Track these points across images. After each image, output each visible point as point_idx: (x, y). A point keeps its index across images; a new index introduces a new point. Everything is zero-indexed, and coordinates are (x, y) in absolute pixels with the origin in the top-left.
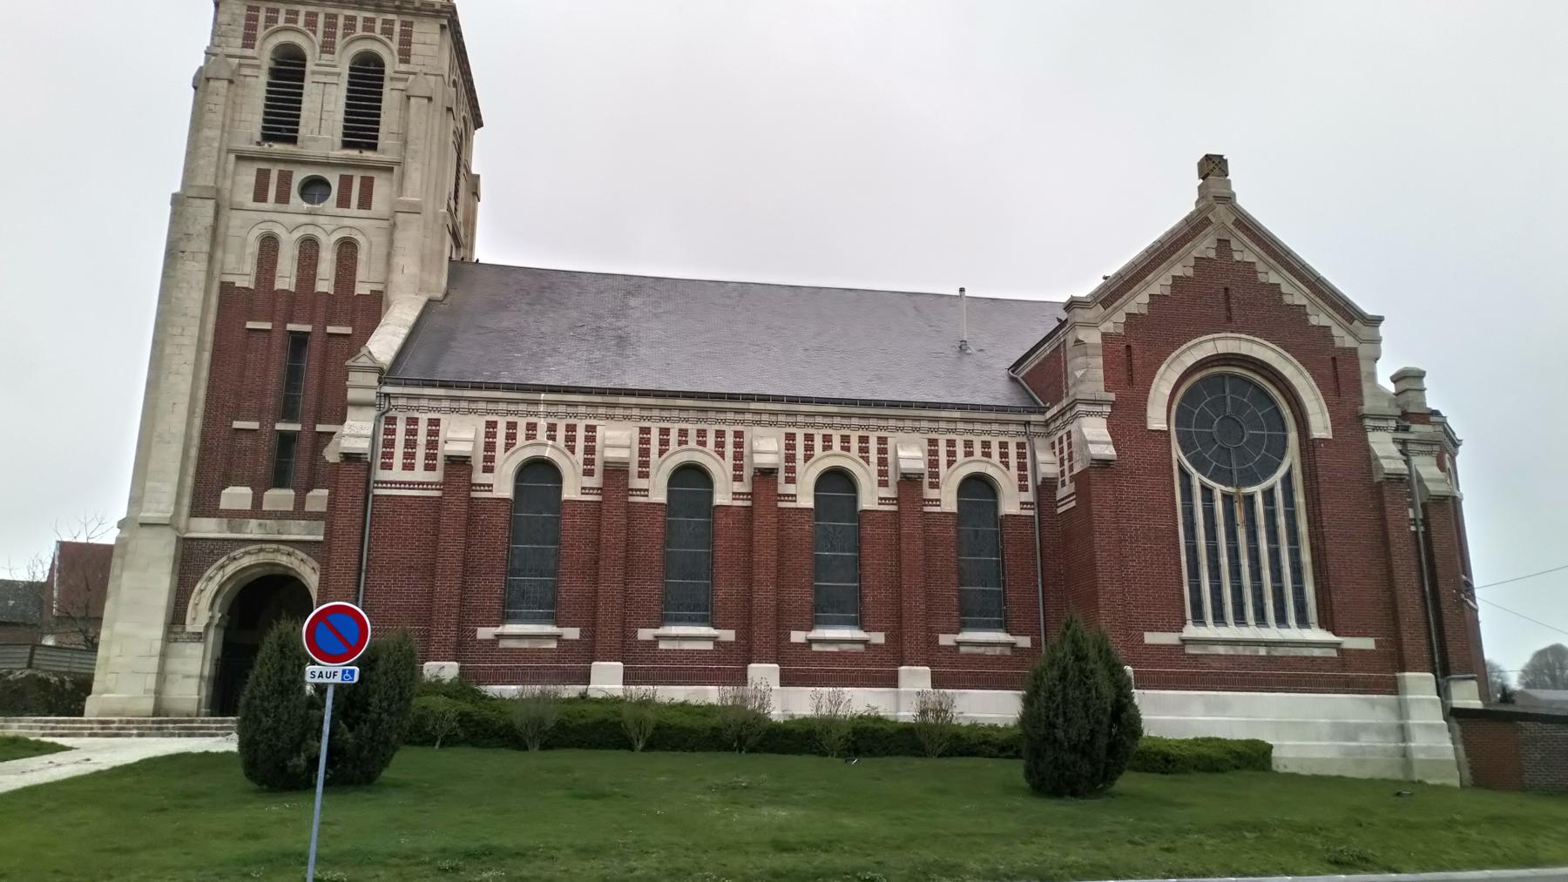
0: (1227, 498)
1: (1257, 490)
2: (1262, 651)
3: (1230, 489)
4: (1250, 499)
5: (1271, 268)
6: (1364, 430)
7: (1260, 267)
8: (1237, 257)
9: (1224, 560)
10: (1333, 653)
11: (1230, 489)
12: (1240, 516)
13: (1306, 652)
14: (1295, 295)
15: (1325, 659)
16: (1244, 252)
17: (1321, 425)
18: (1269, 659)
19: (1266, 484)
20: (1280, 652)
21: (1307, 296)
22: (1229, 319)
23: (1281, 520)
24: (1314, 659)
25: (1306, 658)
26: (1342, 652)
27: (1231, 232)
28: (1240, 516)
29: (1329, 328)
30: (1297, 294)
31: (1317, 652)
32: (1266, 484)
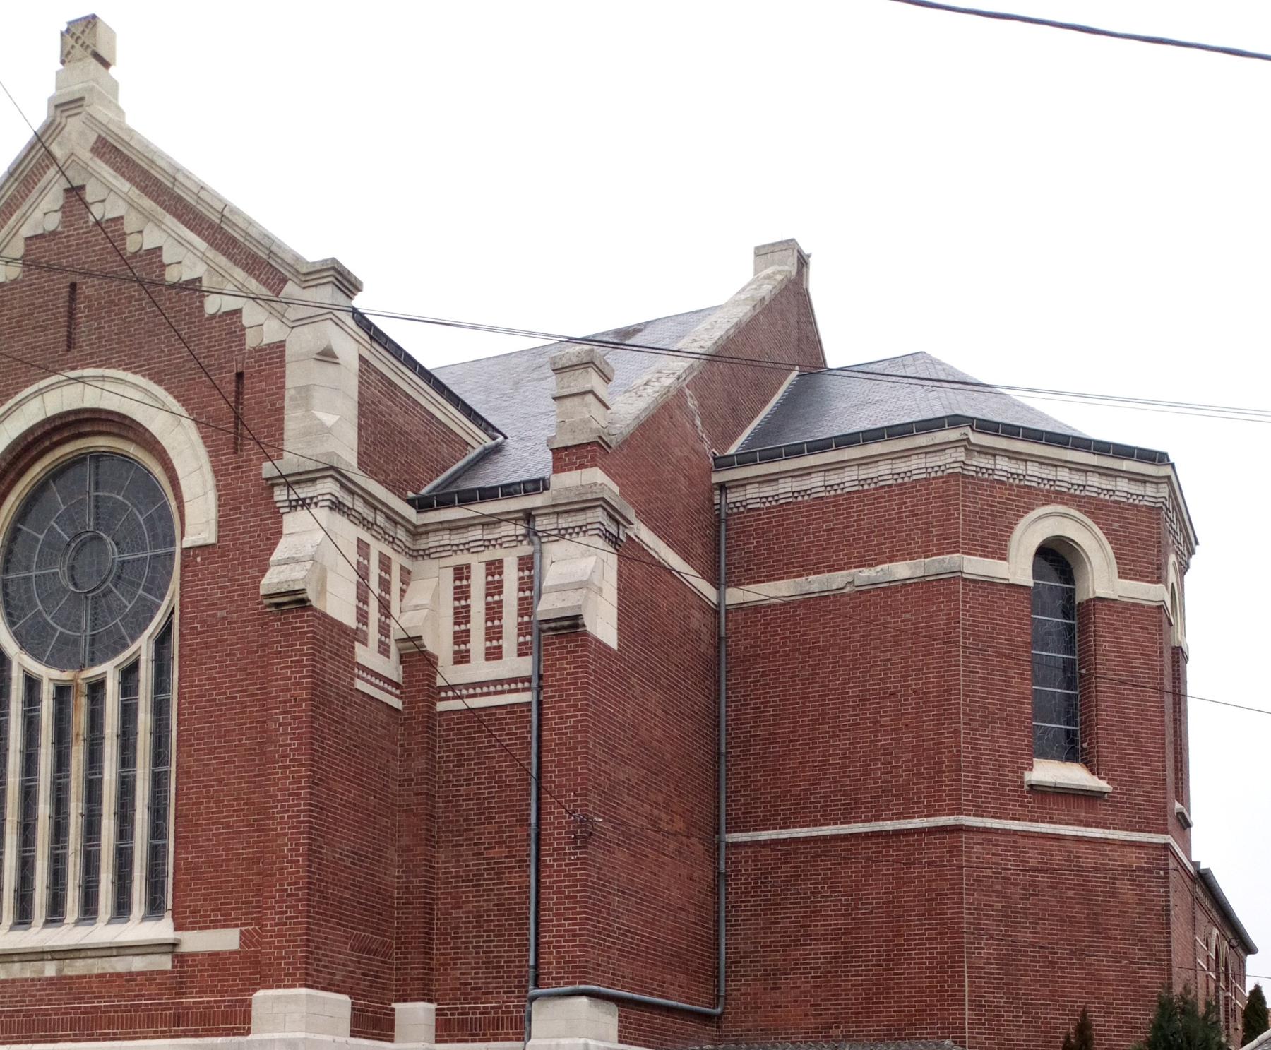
0: (62, 692)
1: (109, 671)
2: (50, 970)
3: (67, 676)
4: (97, 688)
5: (148, 217)
6: (278, 516)
7: (131, 224)
8: (97, 212)
9: (44, 809)
10: (165, 963)
11: (67, 676)
12: (79, 721)
13: (120, 965)
14: (186, 258)
15: (149, 976)
16: (111, 197)
17: (200, 522)
18: (61, 982)
19: (123, 657)
20: (77, 968)
21: (204, 259)
22: (70, 344)
23: (144, 720)
24: (130, 976)
25: (119, 975)
26: (181, 959)
27: (85, 168)
28: (79, 721)
29: (237, 312)
30: (189, 259)
31: (138, 964)
32: (123, 657)
